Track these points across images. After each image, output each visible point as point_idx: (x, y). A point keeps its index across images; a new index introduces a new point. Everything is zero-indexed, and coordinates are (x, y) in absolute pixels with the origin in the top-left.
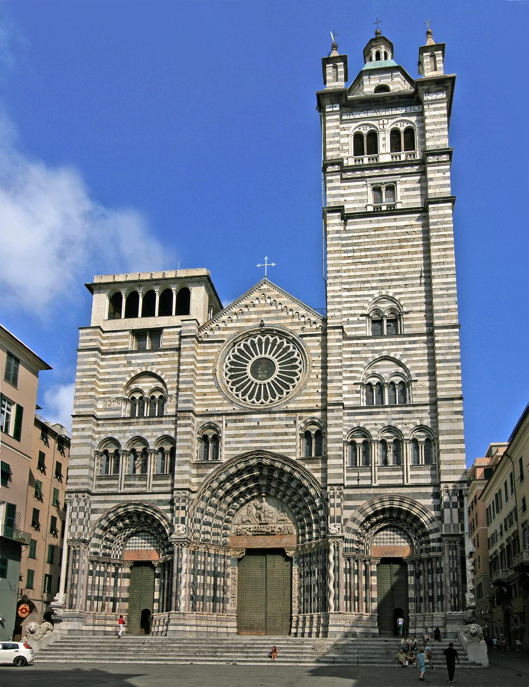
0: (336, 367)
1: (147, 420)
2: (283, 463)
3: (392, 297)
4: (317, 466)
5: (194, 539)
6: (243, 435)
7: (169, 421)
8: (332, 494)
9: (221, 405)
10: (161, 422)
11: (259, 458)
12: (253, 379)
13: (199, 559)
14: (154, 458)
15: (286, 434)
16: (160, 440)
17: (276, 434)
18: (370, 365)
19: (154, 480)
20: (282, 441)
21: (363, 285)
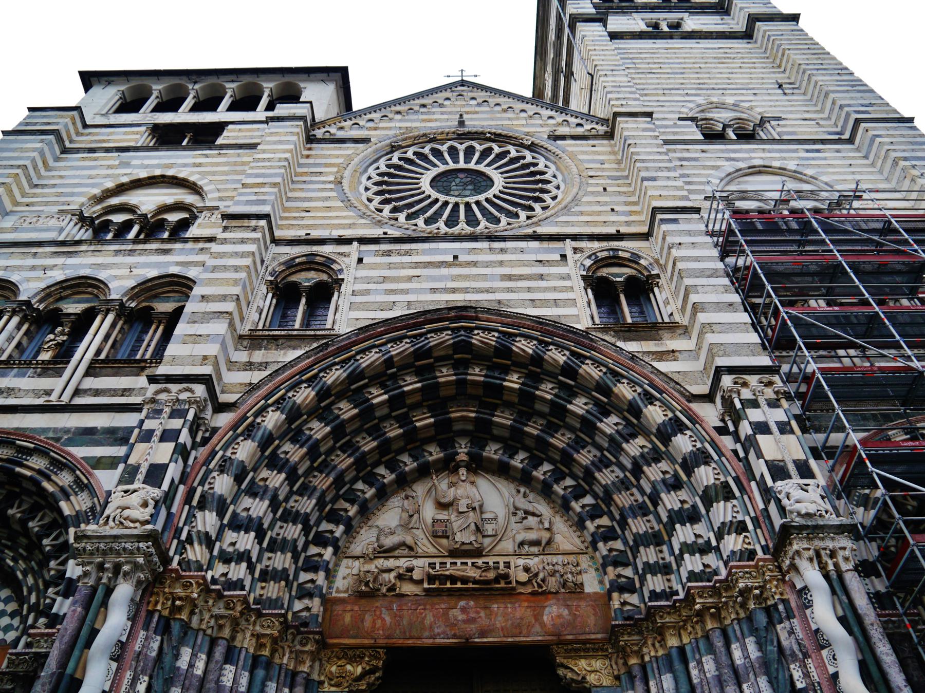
0: (654, 161)
1: (130, 247)
2: (541, 342)
3: (734, 105)
4: (657, 345)
5: (179, 564)
6: (410, 279)
7: (194, 249)
8: (746, 394)
9: (350, 226)
10: (166, 252)
11: (458, 329)
12: (435, 195)
13: (183, 663)
14: (113, 325)
15: (541, 277)
16: (150, 289)
17: (510, 277)
18: (732, 176)
19: (87, 374)
20: (529, 290)
21: (665, 92)
